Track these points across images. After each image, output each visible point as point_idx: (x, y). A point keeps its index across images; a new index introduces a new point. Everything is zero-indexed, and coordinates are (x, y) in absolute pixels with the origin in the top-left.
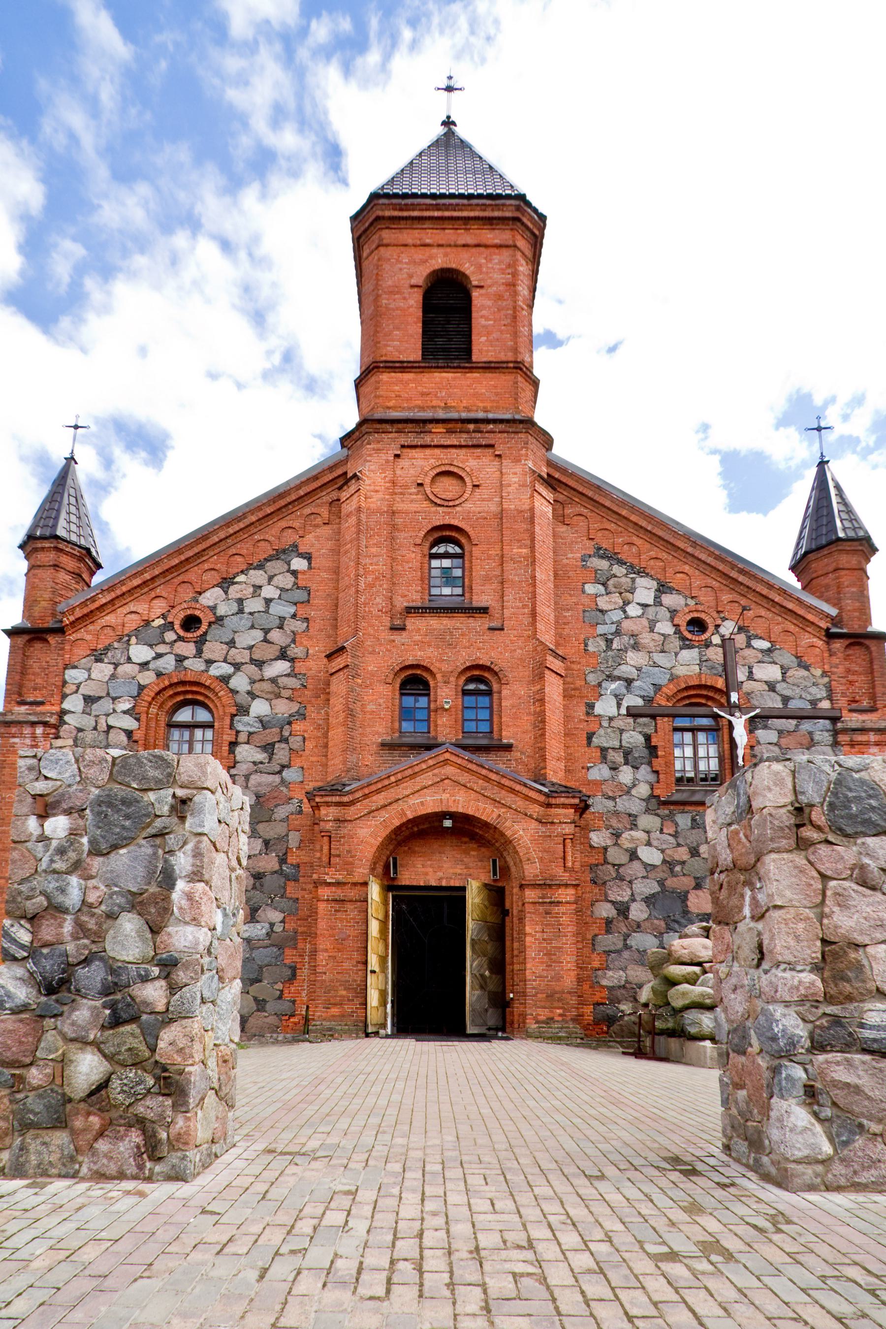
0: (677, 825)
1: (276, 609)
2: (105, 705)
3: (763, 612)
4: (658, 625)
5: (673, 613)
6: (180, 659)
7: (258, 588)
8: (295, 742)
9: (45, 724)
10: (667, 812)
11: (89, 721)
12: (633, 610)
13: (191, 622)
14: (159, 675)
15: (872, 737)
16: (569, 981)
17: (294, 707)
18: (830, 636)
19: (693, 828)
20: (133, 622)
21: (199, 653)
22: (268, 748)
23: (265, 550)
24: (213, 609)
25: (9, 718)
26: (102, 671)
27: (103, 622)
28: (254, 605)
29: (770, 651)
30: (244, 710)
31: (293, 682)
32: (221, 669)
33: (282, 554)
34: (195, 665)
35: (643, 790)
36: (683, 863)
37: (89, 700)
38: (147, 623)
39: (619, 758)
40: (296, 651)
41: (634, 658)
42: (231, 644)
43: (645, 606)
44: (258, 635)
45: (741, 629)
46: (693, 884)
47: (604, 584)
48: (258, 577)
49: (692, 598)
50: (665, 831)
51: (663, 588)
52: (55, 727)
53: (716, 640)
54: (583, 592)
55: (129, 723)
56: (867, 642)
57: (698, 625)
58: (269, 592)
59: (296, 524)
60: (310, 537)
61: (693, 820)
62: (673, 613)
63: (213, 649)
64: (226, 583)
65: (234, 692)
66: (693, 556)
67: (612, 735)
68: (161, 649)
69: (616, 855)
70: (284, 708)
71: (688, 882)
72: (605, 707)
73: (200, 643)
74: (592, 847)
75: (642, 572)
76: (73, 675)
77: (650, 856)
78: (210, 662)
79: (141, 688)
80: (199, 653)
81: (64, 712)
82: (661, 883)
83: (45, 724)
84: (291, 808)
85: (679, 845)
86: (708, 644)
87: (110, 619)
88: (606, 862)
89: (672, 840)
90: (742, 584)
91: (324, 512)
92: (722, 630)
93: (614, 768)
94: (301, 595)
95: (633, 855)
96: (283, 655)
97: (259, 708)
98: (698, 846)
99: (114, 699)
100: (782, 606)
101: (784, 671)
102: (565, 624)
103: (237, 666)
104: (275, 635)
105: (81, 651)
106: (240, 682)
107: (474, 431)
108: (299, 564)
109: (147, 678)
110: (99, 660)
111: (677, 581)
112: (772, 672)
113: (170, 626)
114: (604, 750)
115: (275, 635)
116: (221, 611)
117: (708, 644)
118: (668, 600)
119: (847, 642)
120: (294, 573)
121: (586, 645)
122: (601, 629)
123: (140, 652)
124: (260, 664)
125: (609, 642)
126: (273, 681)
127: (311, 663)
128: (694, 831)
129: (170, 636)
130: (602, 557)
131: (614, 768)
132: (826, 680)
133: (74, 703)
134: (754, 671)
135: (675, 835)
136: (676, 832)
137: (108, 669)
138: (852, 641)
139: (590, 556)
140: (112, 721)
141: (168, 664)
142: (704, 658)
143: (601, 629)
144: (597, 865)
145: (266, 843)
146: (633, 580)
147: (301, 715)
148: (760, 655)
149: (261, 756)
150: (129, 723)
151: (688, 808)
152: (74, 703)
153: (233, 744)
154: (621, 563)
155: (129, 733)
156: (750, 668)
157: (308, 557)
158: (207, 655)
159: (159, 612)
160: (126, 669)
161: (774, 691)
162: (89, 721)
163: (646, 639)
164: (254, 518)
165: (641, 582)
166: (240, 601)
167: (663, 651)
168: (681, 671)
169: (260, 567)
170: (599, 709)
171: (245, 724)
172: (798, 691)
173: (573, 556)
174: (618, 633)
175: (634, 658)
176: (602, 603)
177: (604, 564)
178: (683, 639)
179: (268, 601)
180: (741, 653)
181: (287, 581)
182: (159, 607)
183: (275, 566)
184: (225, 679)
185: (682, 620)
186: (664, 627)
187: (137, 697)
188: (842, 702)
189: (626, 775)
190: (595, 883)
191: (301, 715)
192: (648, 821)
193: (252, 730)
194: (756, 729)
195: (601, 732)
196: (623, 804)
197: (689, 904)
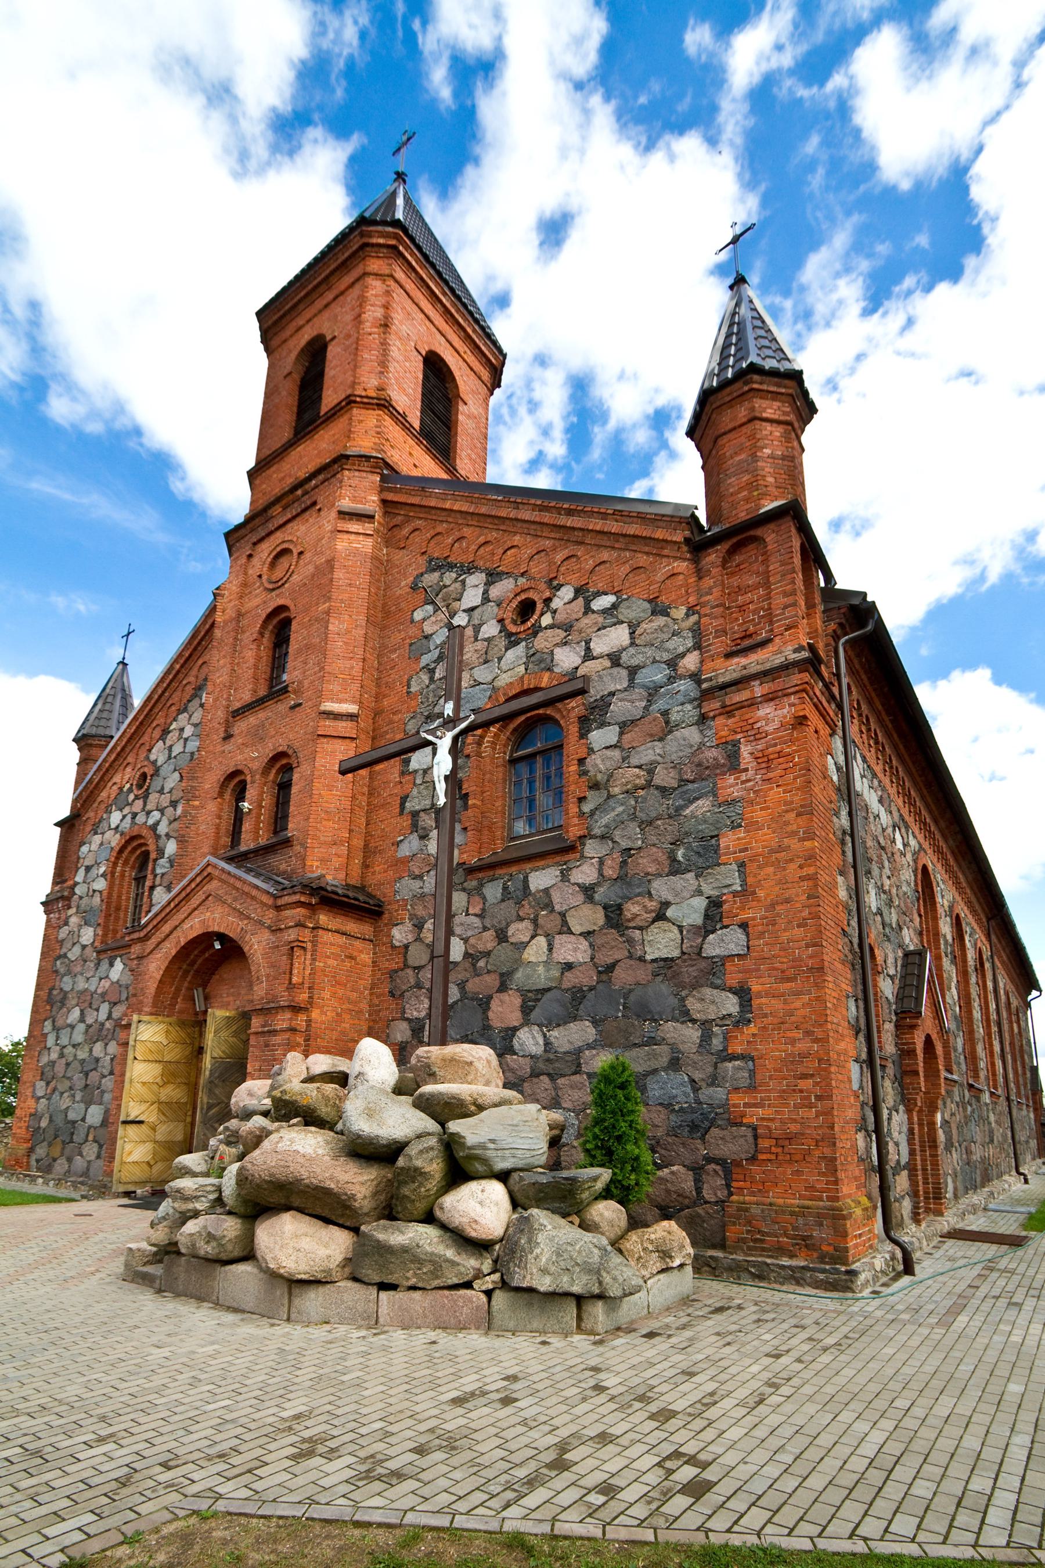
0: (484, 899)
3: (605, 555)
4: (484, 628)
6: (134, 815)
10: (474, 883)
15: (758, 689)
19: (503, 900)
23: (189, 690)
24: (154, 762)
27: (99, 799)
28: (177, 749)
29: (614, 606)
30: (161, 852)
34: (141, 819)
36: (488, 954)
38: (121, 789)
39: (428, 821)
43: (471, 610)
45: (578, 592)
46: (497, 983)
47: (433, 603)
48: (183, 717)
49: (522, 575)
50: (471, 911)
54: (412, 621)
56: (758, 532)
57: (526, 609)
61: (505, 888)
64: (166, 732)
66: (517, 520)
67: (425, 792)
68: (126, 810)
71: (492, 981)
73: (146, 797)
74: (393, 947)
75: (470, 569)
78: (148, 813)
85: (485, 929)
88: (406, 966)
89: (476, 921)
90: (574, 529)
92: (556, 604)
98: (508, 925)
100: (625, 536)
102: (392, 668)
103: (162, 811)
106: (162, 829)
107: (303, 495)
114: (415, 814)
117: (536, 630)
118: (495, 592)
119: (723, 548)
121: (409, 686)
122: (425, 660)
125: (432, 671)
128: (503, 905)
129: (131, 797)
130: (434, 570)
132: (694, 618)
134: (592, 645)
135: (481, 916)
136: (483, 910)
138: (734, 540)
139: (422, 574)
141: (127, 823)
142: (531, 652)
143: (425, 660)
144: (396, 971)
146: (463, 582)
148: (601, 619)
151: (499, 872)
154: (451, 566)
156: (588, 642)
161: (619, 665)
164: (178, 666)
166: (170, 748)
167: (486, 662)
168: (504, 680)
169: (185, 710)
172: (650, 652)
176: (428, 628)
177: (431, 579)
178: (509, 635)
179: (186, 740)
180: (578, 626)
184: (154, 827)
186: (491, 629)
190: (393, 996)
193: (164, 871)
194: (589, 731)
195: (415, 792)
197: (490, 1014)
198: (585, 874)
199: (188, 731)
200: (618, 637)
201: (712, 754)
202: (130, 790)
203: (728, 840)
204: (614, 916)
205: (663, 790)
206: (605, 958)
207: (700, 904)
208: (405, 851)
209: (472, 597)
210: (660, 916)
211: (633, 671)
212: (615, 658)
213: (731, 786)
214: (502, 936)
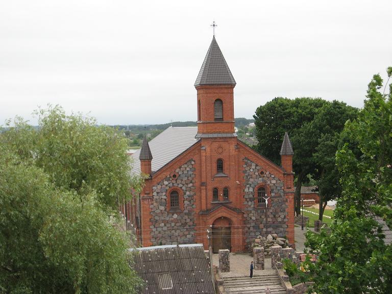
1: (190, 173)
2: (161, 194)
5: (258, 170)
6: (173, 184)
7: (186, 168)
8: (194, 199)
9: (151, 199)
11: (158, 197)
12: (252, 170)
13: (175, 176)
14: (170, 187)
16: (241, 244)
17: (194, 193)
18: (284, 174)
20: (164, 177)
21: (176, 182)
22: (190, 201)
24: (178, 173)
25: (144, 198)
26: (159, 187)
30: (185, 194)
31: (192, 188)
32: (180, 185)
33: (190, 161)
35: (252, 206)
37: (158, 193)
39: (248, 200)
40: (193, 181)
41: (251, 180)
42: (182, 180)
44: (186, 178)
48: (186, 166)
51: (257, 165)
52: (152, 199)
53: (265, 176)
55: (165, 197)
57: (262, 173)
58: (188, 169)
59: (192, 154)
60: (195, 157)
62: (258, 170)
63: (179, 181)
64: (180, 168)
65: (183, 190)
69: (248, 219)
70: (192, 193)
72: (246, 190)
76: (154, 188)
77: (254, 218)
79: (167, 190)
80: (176, 182)
81: (153, 196)
82: (255, 223)
83: (151, 199)
84: (194, 213)
86: (264, 177)
87: (160, 176)
91: (197, 152)
93: (248, 202)
94: (193, 169)
95: (251, 218)
96: (191, 182)
97: (188, 193)
99: (162, 193)
101: (276, 181)
103: (183, 185)
104: (190, 178)
105: (155, 183)
106: (184, 188)
108: (193, 163)
109: (167, 188)
110: (158, 185)
111: (259, 164)
112: (274, 182)
113: (171, 177)
115: (190, 178)
116: (180, 173)
120: (192, 165)
123: (166, 183)
124: (187, 184)
125: (247, 177)
126: (190, 188)
127: (196, 184)
129: (171, 179)
131: (248, 202)
133: (155, 194)
137: (160, 186)
140: (162, 197)
141: (171, 185)
145: (191, 220)
147: (195, 194)
149: (189, 203)
150: (165, 197)
152: (155, 194)
153: (184, 201)
155: (165, 200)
157: (194, 161)
158: (178, 183)
159: (168, 174)
160: (163, 186)
162: (158, 197)
163: (254, 176)
165: (253, 164)
168: (259, 182)
169: (186, 164)
170: (245, 191)
171: (186, 197)
173: (241, 160)
174: (249, 175)
175: (251, 180)
179: (188, 171)
181: (191, 166)
182: (169, 173)
183: (189, 163)
184: (181, 188)
185: (259, 172)
187: (166, 192)
188: (286, 187)
189: (250, 203)
191: (195, 194)
192: (253, 212)
196: (249, 209)
198: (271, 211)
199: (188, 169)
200: (274, 182)
201: (285, 200)
202: (171, 177)
203: (286, 210)
204: (275, 216)
205: (280, 203)
206: (274, 221)
207: (284, 216)
208: (245, 203)
209: (253, 167)
210: (279, 217)
211: (276, 187)
212: (274, 184)
213: (287, 204)
214: (261, 217)
